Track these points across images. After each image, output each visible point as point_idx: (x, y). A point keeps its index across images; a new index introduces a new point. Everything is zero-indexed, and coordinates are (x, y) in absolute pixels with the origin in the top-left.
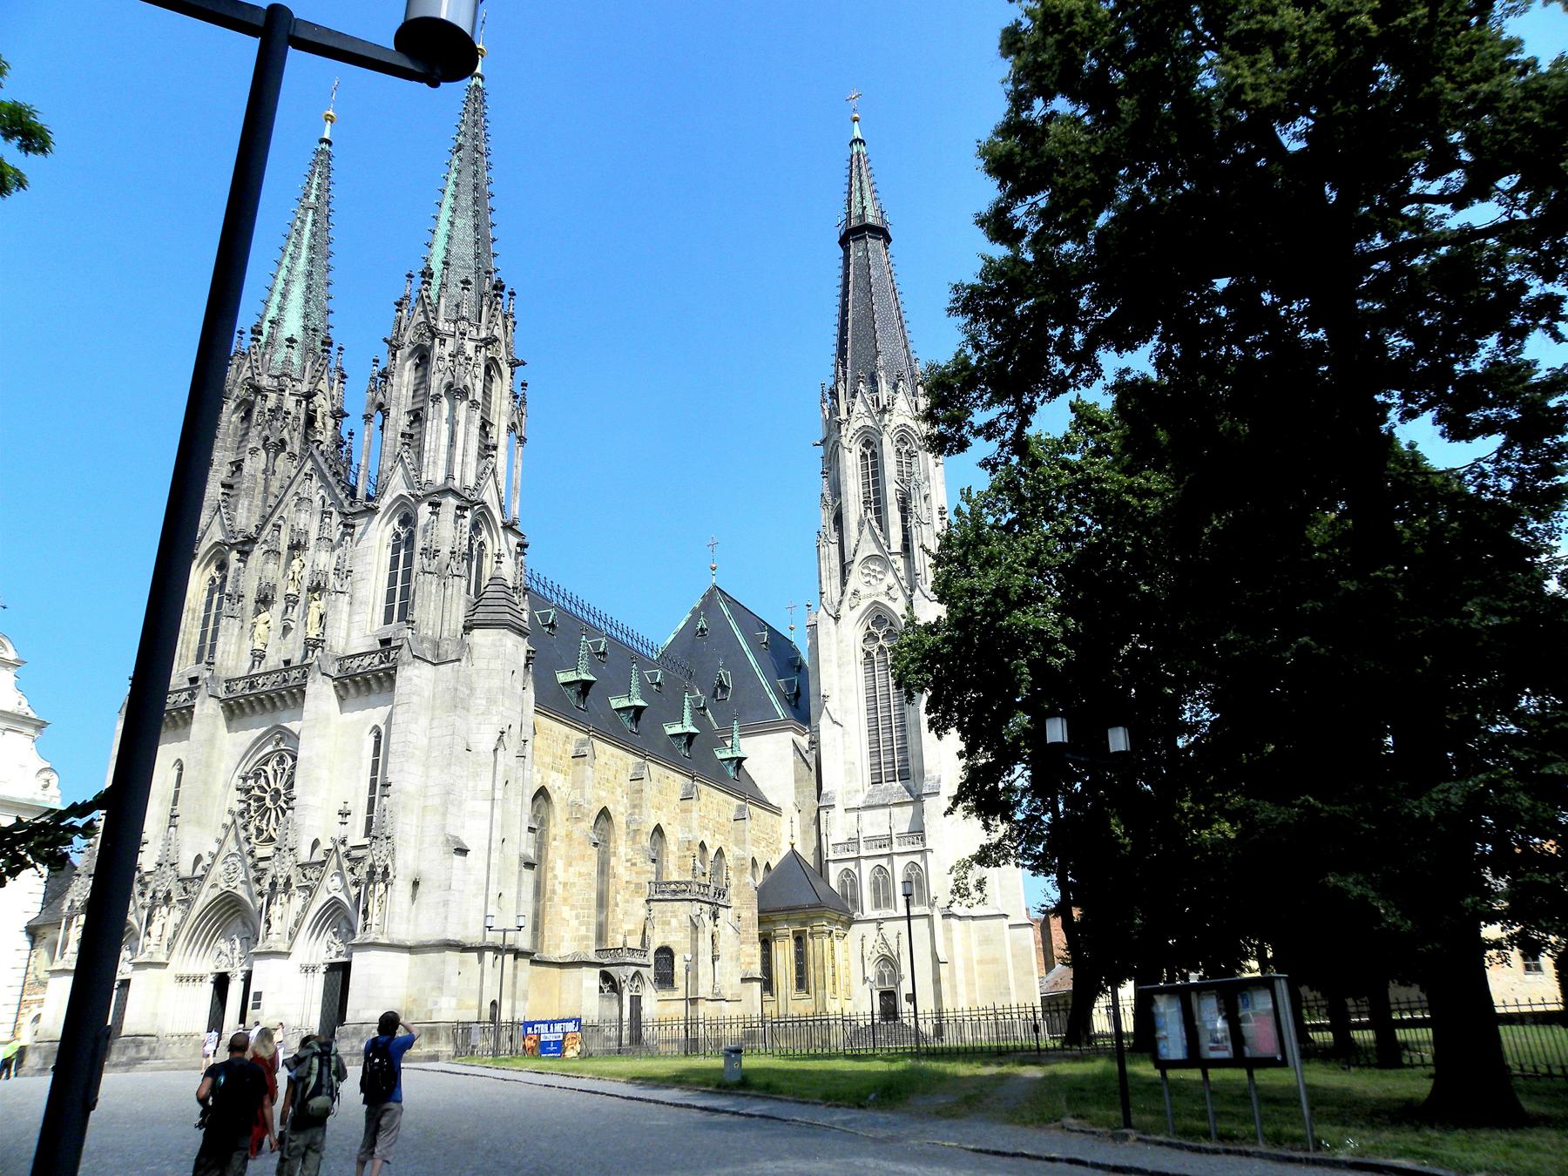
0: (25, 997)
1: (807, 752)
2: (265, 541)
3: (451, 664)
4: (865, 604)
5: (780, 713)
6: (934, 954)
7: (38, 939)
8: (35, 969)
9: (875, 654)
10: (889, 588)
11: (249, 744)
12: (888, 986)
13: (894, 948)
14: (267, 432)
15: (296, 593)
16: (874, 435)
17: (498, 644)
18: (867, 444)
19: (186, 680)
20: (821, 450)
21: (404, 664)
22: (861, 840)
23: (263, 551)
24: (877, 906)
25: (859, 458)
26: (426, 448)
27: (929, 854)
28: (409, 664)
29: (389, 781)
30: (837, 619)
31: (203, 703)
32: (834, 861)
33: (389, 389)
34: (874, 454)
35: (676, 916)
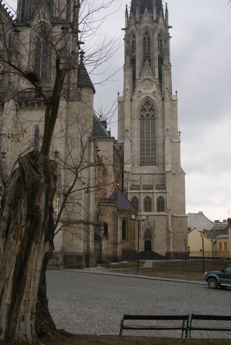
1: (118, 151)
3: (75, 102)
4: (143, 97)
5: (107, 135)
6: (167, 229)
12: (148, 239)
13: (152, 226)
16: (150, 31)
18: (147, 33)
20: (124, 32)
22: (142, 186)
24: (146, 210)
25: (143, 38)
27: (167, 193)
29: (58, 151)
32: (130, 193)
34: (149, 38)
35: (108, 212)
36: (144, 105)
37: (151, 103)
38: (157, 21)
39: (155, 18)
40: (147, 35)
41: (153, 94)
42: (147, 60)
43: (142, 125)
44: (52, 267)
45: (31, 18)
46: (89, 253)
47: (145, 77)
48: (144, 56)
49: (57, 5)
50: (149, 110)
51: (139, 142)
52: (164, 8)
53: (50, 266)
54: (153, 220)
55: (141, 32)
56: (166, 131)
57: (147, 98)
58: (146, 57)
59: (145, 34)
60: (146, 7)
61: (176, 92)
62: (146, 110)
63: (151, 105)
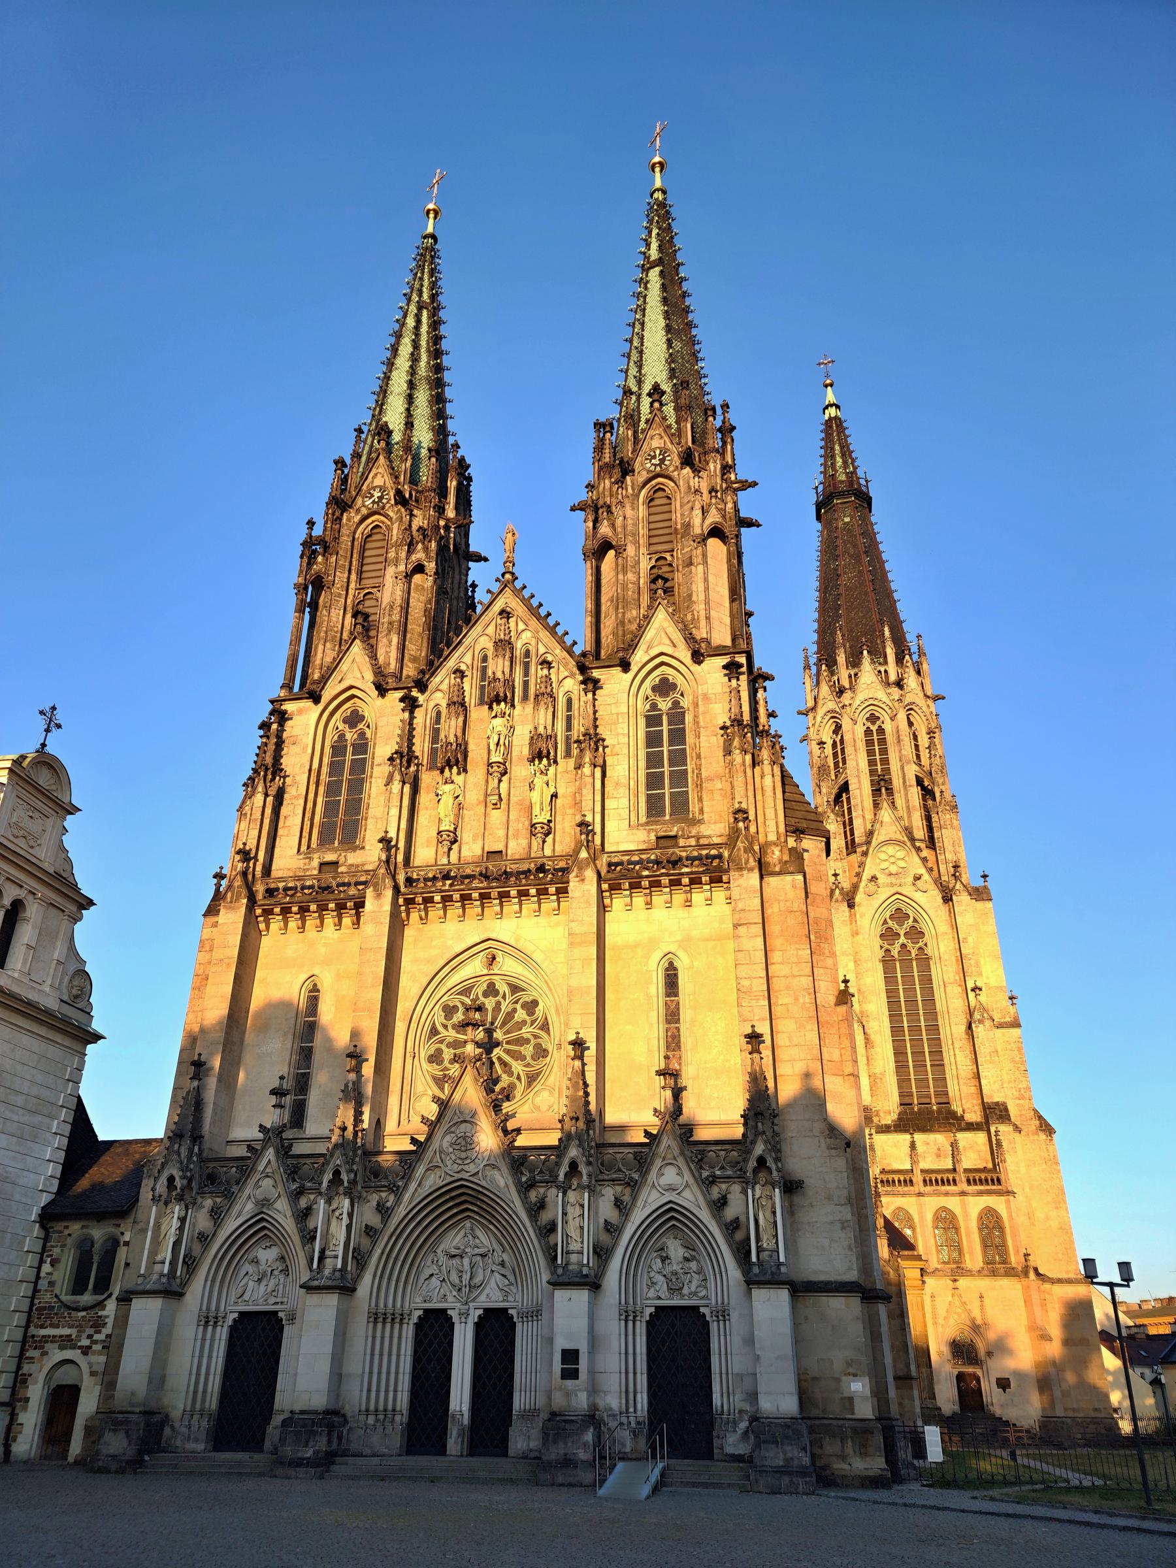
0: (32, 1330)
2: (438, 690)
4: (884, 893)
7: (55, 1236)
8: (51, 1284)
9: (895, 953)
10: (918, 878)
11: (442, 963)
14: (419, 555)
15: (502, 761)
17: (817, 860)
18: (873, 718)
19: (315, 863)
21: (741, 869)
23: (432, 704)
26: (694, 598)
28: (751, 870)
30: (851, 906)
31: (379, 895)
33: (619, 521)
34: (881, 731)
36: (888, 920)
37: (910, 912)
38: (899, 684)
39: (893, 677)
40: (873, 723)
41: (914, 884)
42: (883, 790)
43: (890, 979)
44: (786, 1480)
45: (632, 646)
46: (890, 1419)
47: (882, 838)
48: (871, 781)
49: (702, 606)
50: (906, 934)
51: (888, 1032)
52: (914, 649)
53: (778, 1475)
54: (979, 1295)
55: (856, 715)
56: (971, 995)
57: (897, 896)
58: (879, 783)
59: (867, 719)
60: (865, 647)
61: (985, 876)
62: (899, 935)
63: (911, 919)
